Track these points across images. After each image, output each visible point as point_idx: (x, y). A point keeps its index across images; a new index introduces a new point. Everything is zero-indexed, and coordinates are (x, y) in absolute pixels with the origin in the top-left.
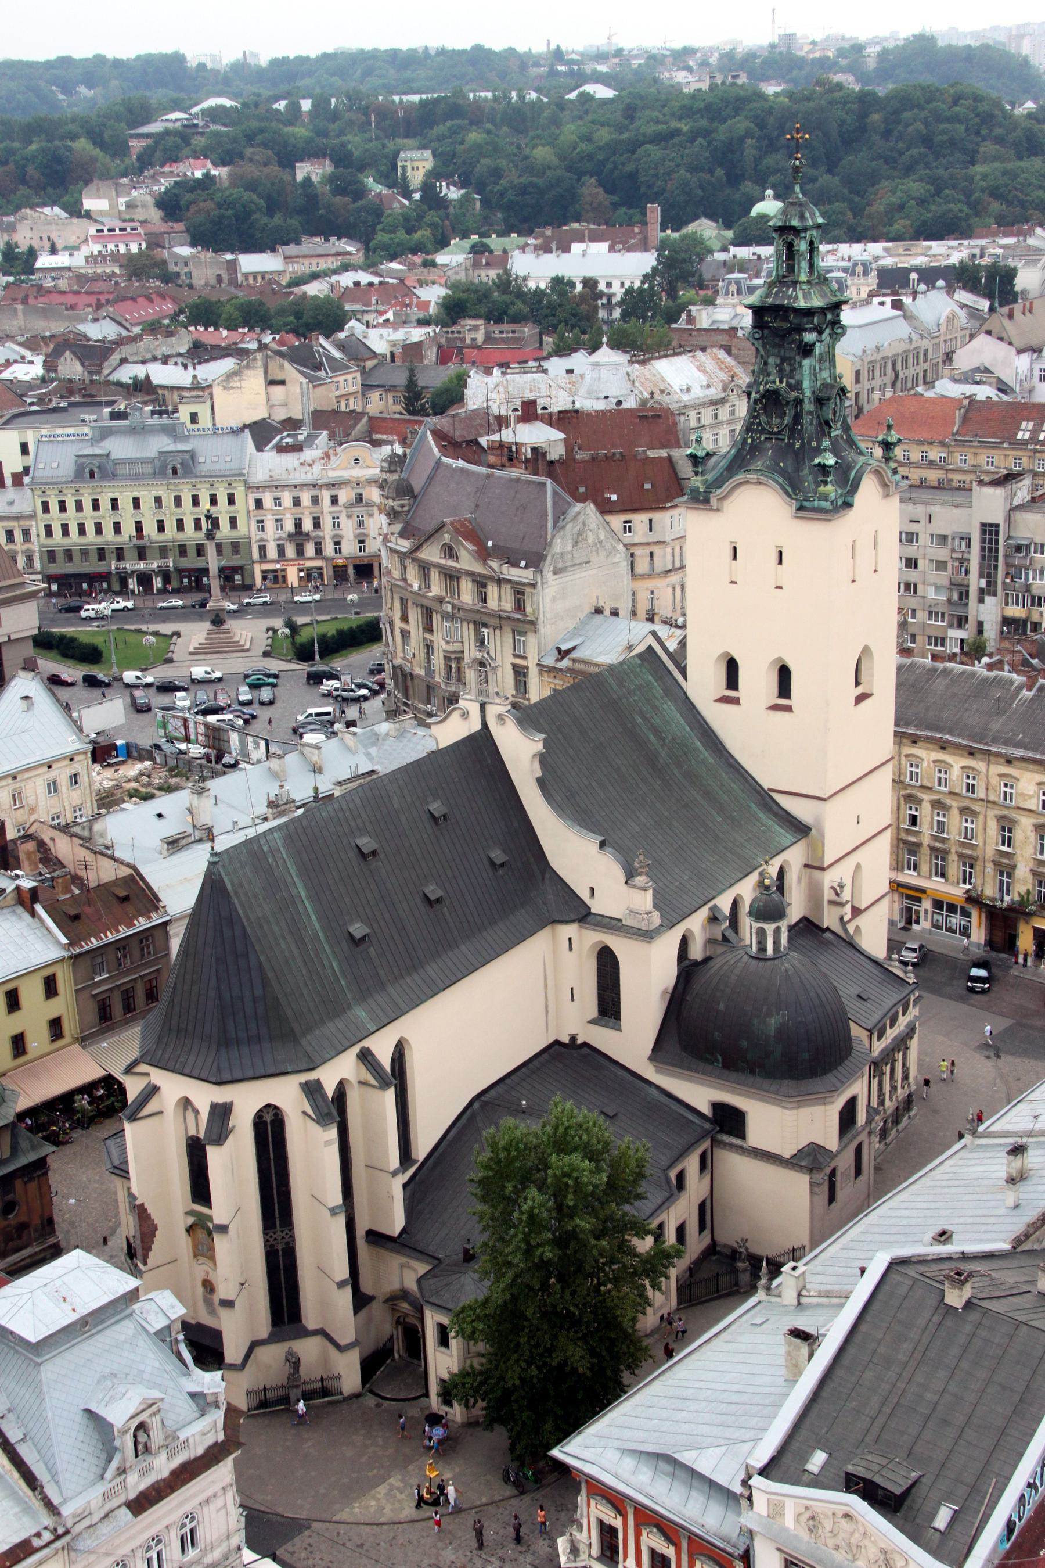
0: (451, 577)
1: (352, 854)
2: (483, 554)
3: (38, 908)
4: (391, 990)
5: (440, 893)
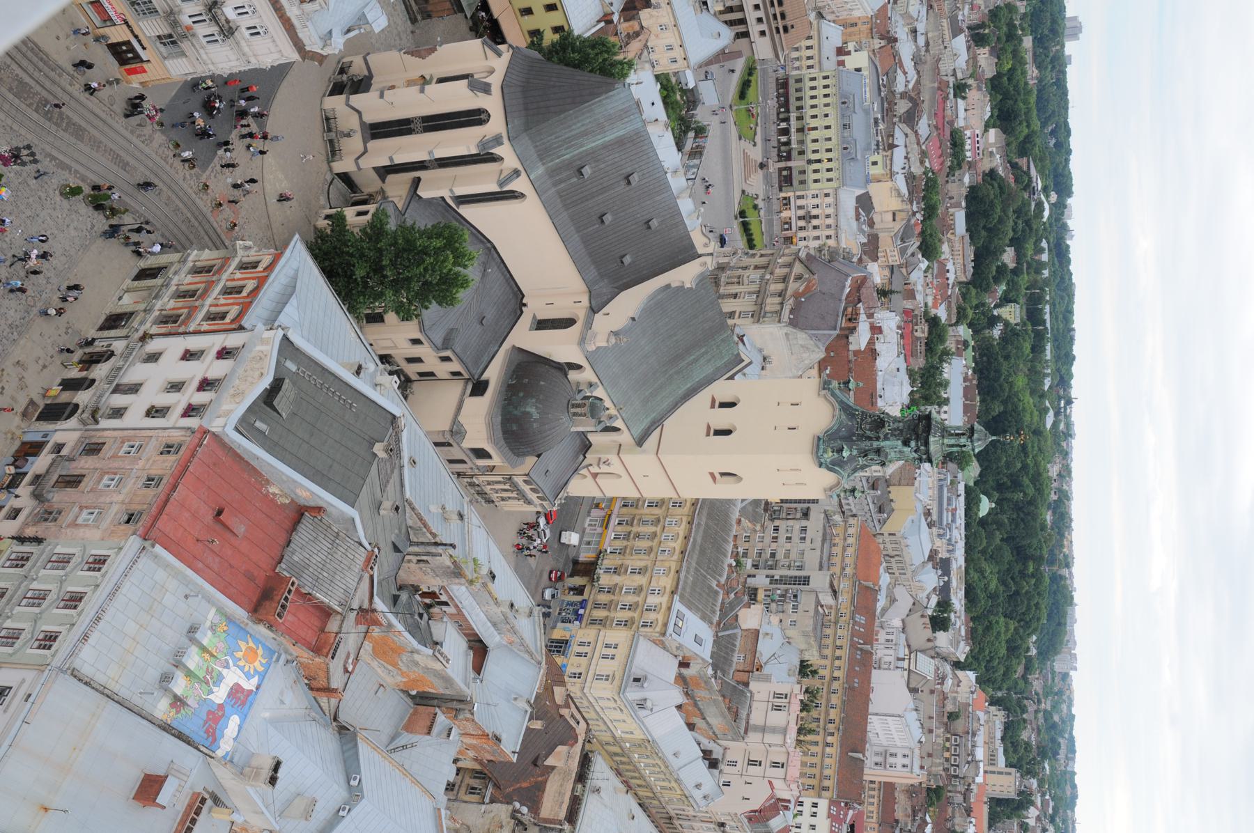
0: (785, 279)
1: (629, 170)
2: (797, 295)
3: (602, 24)
4: (553, 190)
5: (607, 223)
